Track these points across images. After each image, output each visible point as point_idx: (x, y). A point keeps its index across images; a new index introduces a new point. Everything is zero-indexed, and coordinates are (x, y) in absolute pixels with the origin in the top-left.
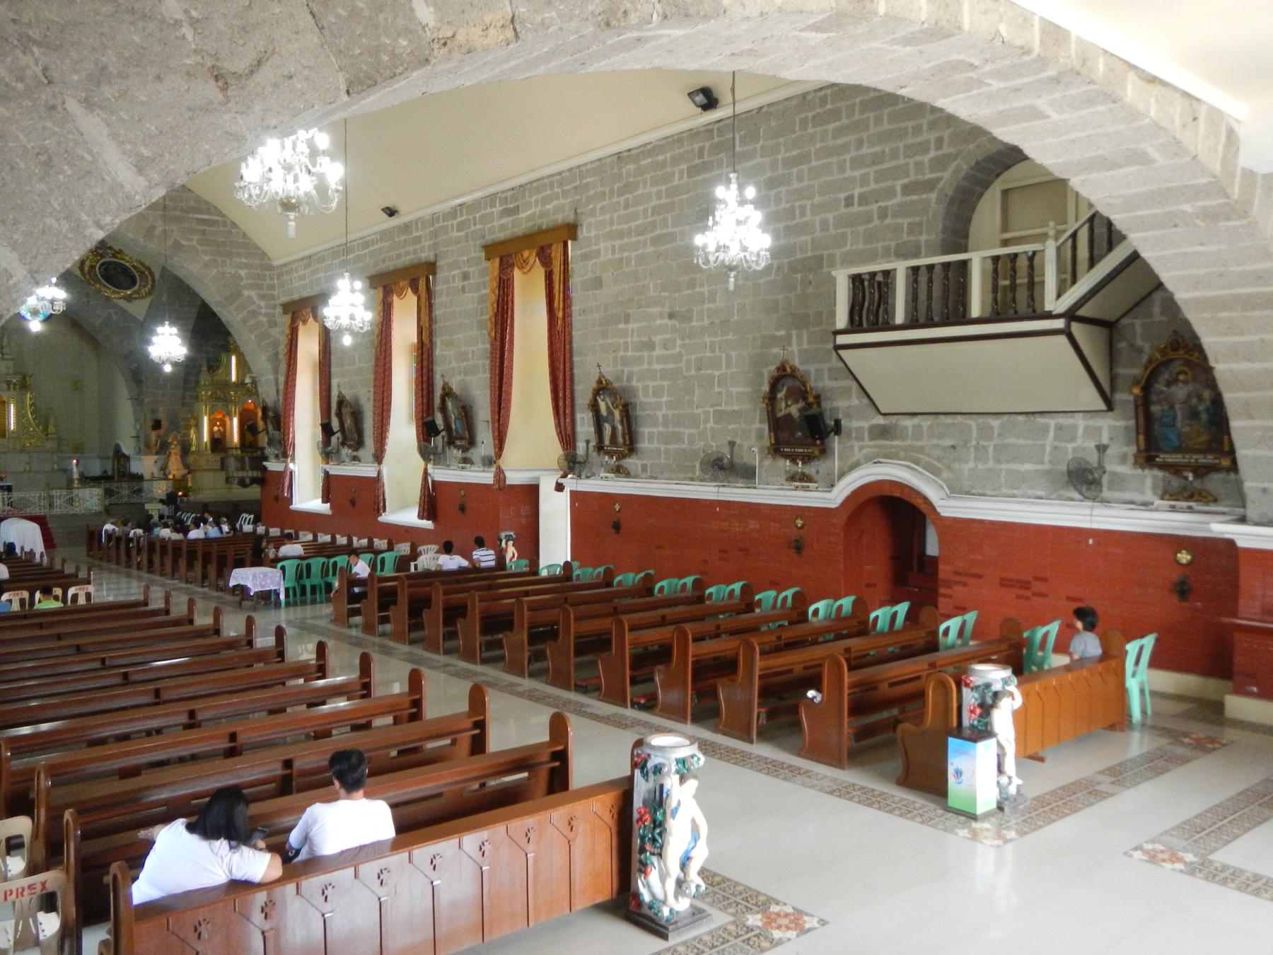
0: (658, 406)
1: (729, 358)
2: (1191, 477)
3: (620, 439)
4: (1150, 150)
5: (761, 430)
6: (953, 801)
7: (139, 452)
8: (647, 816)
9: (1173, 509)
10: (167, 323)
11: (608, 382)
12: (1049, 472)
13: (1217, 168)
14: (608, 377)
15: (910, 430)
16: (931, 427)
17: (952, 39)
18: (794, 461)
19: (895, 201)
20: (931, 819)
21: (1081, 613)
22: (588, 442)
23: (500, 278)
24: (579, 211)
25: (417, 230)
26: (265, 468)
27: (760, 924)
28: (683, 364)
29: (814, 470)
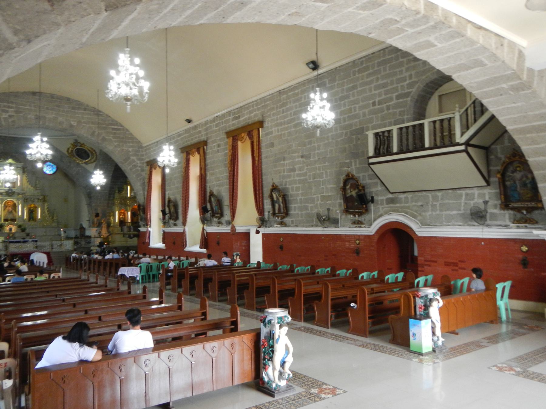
0: (298, 195)
1: (326, 173)
2: (525, 212)
3: (282, 210)
4: (483, 59)
5: (340, 203)
6: (412, 348)
7: (90, 227)
8: (266, 343)
9: (518, 227)
11: (277, 186)
12: (463, 214)
13: (515, 66)
14: (276, 184)
15: (403, 199)
16: (412, 197)
17: (383, 6)
18: (354, 215)
19: (393, 102)
20: (402, 355)
21: (475, 271)
22: (269, 212)
23: (233, 146)
25: (200, 128)
26: (139, 231)
27: (317, 392)
28: (307, 177)
29: (363, 219)
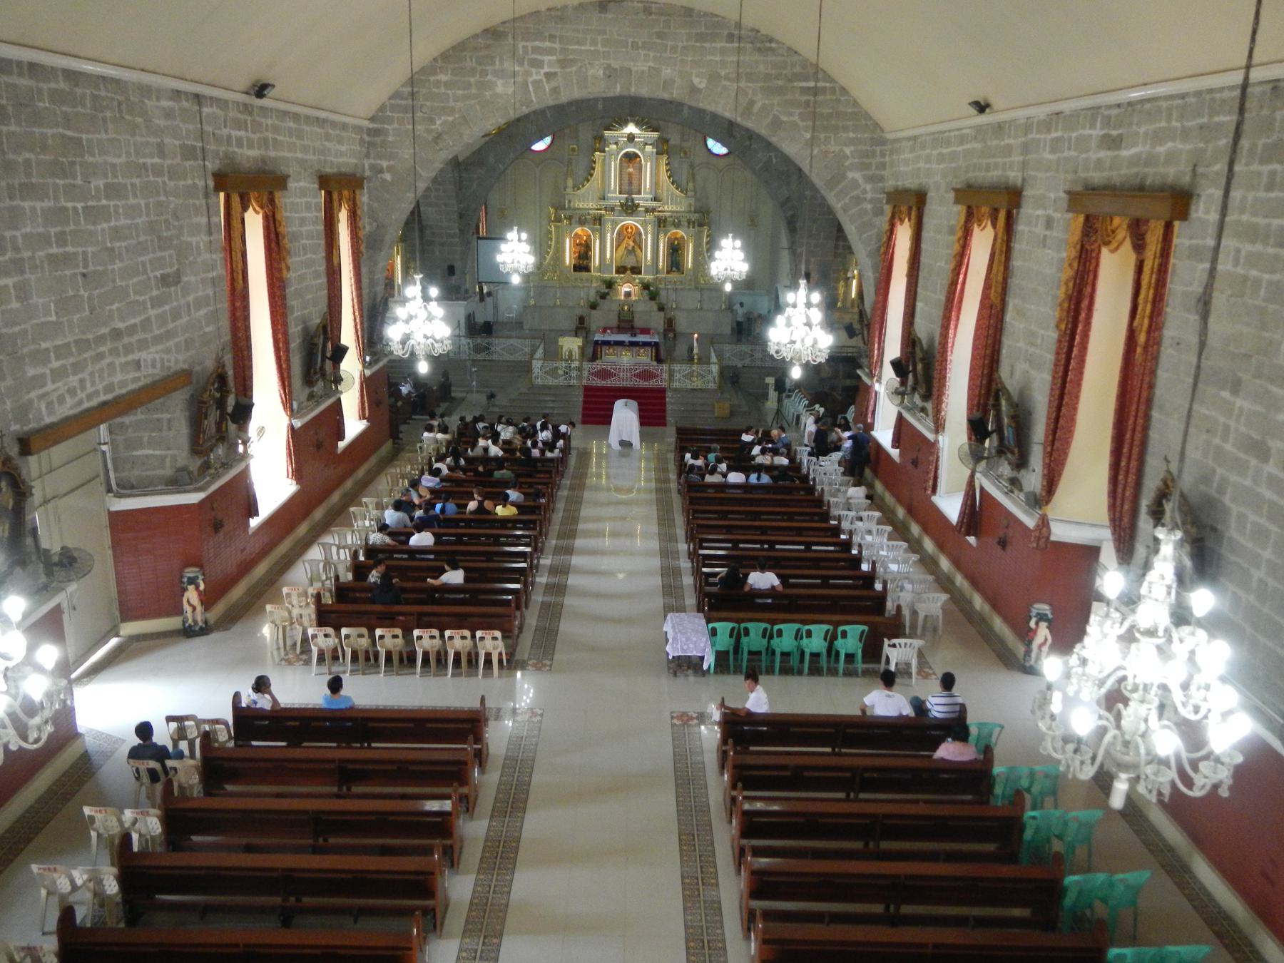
10: (730, 235)
23: (1082, 246)
24: (1200, 170)
26: (859, 377)
